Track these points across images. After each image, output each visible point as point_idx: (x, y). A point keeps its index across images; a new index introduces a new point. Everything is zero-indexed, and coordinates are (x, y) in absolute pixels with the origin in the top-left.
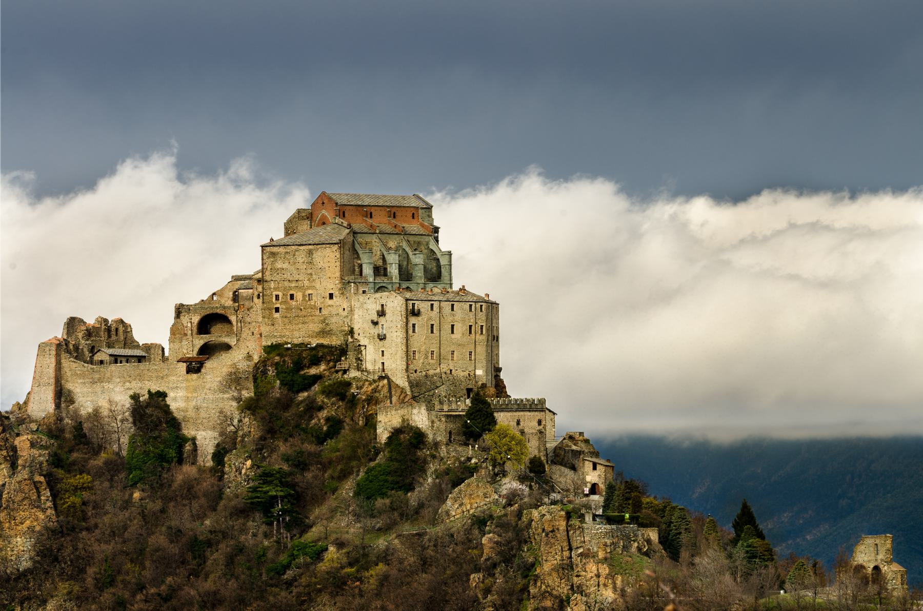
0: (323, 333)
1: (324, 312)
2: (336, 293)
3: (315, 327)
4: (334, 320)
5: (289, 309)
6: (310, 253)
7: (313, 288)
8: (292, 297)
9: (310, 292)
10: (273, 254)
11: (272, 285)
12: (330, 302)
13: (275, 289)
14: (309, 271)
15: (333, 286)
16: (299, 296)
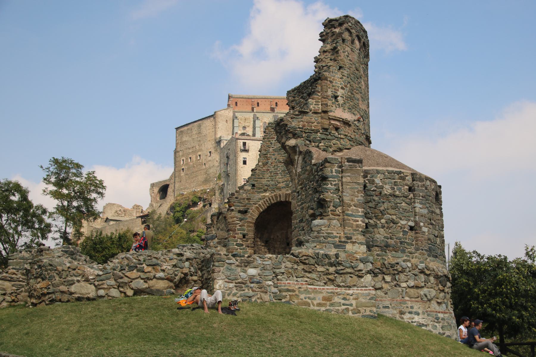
0: (206, 181)
1: (207, 166)
2: (213, 150)
3: (201, 178)
4: (211, 171)
5: (188, 169)
6: (199, 126)
7: (200, 150)
8: (190, 158)
9: (199, 153)
10: (182, 132)
11: (181, 153)
12: (210, 158)
13: (183, 156)
14: (199, 139)
15: (212, 146)
16: (194, 158)
